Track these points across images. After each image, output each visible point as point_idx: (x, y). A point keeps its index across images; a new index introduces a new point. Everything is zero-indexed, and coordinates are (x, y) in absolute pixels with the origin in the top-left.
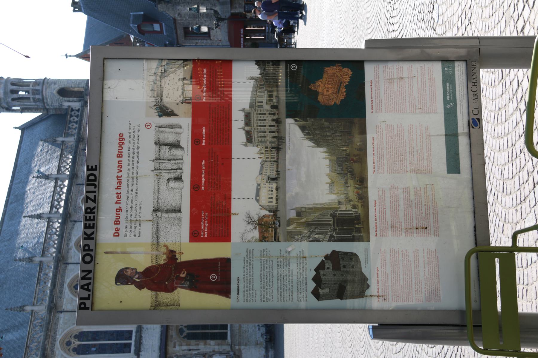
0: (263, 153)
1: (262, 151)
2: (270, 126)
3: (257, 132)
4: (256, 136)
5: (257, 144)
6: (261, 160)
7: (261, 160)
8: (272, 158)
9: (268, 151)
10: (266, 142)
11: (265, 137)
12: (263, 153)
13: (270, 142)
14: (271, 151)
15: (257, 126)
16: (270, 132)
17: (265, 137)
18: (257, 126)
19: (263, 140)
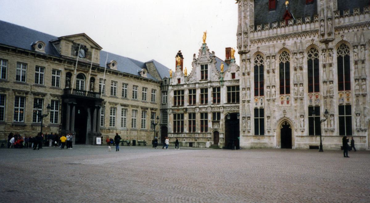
0: (204, 75)
1: (212, 75)
2: (345, 110)
3: (313, 49)
4: (290, 43)
5: (253, 48)
6: (170, 64)
7: (170, 64)
8: (178, 117)
9: (217, 98)
10: (259, 91)
11: (285, 88)
12: (204, 75)
13: (259, 113)
14: (216, 116)
15: (343, 45)
16: (314, 110)
17: (285, 88)
18: (343, 45)
19: (272, 79)
